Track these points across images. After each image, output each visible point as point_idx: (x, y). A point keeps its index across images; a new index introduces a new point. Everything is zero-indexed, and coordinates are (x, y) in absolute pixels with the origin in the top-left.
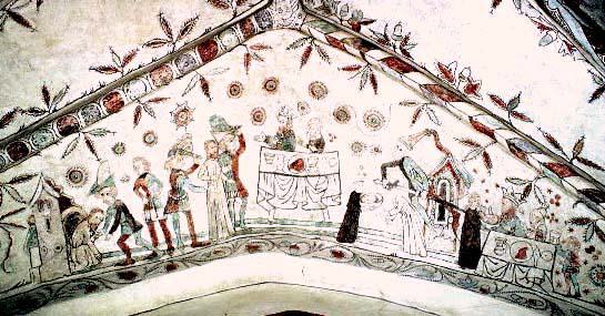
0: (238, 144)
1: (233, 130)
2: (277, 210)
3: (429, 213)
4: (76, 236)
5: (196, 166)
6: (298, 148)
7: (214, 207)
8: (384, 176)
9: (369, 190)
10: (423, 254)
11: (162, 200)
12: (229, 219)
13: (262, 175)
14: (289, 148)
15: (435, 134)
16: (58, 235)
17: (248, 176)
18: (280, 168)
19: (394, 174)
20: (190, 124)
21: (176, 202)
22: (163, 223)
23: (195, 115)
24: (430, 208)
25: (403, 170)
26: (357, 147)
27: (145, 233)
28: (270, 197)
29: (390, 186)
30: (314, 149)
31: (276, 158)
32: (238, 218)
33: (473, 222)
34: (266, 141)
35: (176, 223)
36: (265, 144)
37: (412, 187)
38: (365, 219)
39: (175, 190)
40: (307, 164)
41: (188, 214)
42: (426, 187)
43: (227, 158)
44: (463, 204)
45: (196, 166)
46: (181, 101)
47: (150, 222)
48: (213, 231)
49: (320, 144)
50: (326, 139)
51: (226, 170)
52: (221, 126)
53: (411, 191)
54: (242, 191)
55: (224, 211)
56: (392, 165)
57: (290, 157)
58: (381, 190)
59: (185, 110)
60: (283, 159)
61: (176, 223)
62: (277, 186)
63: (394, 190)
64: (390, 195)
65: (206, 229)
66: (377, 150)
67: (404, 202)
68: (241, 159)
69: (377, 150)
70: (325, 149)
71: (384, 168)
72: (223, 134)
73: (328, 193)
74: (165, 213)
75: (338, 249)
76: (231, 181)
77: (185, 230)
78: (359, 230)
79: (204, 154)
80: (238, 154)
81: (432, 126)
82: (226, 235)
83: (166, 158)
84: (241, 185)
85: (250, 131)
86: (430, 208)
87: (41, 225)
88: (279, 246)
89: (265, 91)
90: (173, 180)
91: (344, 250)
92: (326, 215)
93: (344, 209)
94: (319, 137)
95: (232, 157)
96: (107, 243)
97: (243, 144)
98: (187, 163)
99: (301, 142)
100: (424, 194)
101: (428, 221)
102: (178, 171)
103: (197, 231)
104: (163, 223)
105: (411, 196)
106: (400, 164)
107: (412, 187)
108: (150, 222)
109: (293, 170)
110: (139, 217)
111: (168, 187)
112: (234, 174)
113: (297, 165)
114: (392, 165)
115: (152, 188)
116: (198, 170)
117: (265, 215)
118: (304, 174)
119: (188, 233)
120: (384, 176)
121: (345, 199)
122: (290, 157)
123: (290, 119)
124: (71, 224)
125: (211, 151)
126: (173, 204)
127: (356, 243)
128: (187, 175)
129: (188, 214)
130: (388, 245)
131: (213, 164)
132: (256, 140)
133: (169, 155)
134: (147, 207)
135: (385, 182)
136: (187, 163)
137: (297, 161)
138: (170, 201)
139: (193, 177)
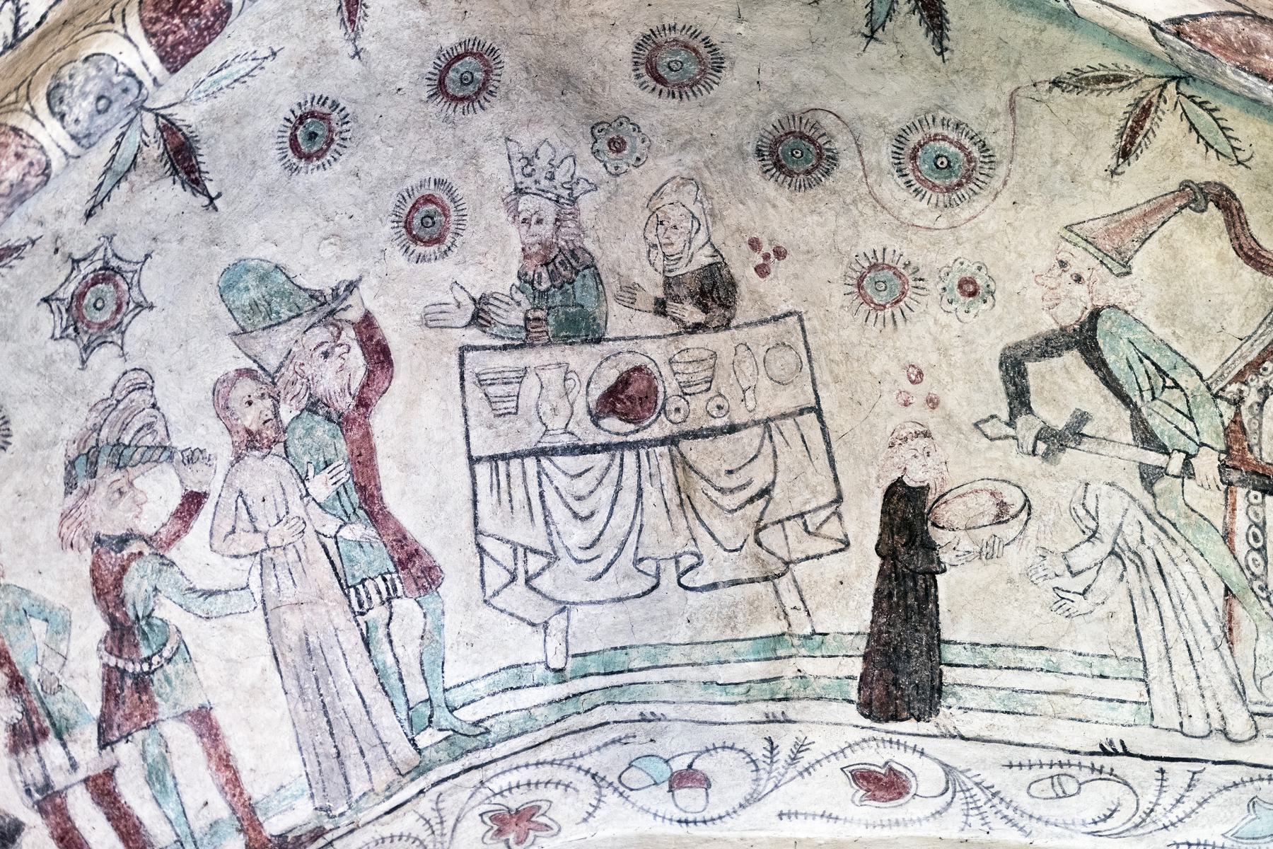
0: (357, 360)
1: (326, 306)
2: (577, 614)
3: (1241, 547)
5: (193, 502)
6: (618, 319)
7: (304, 666)
8: (1019, 399)
9: (966, 470)
10: (1239, 724)
11: (84, 695)
12: (379, 704)
13: (483, 470)
14: (582, 329)
15: (1224, 200)
17: (424, 492)
18: (557, 424)
19: (1064, 386)
20: (139, 327)
21: (142, 683)
22: (103, 789)
23: (152, 283)
24: (1241, 524)
25: (1097, 364)
26: (881, 285)
28: (535, 563)
29: (1055, 441)
30: (692, 314)
31: (531, 382)
32: (417, 691)
34: (479, 318)
35: (157, 775)
36: (474, 336)
37: (1147, 438)
38: (965, 599)
39: (122, 633)
40: (668, 386)
41: (203, 720)
42: (1211, 422)
43: (323, 430)
45: (193, 502)
46: (83, 239)
47: (49, 800)
49: (714, 292)
50: (742, 268)
51: (321, 487)
52: (266, 298)
53: (1154, 458)
54: (413, 566)
55: (351, 672)
56: (1049, 346)
57: (592, 368)
58: (1009, 461)
59: (107, 274)
60: (560, 382)
61: (157, 775)
62: (560, 514)
63: (1069, 457)
64: (1054, 483)
65: (292, 766)
66: (969, 288)
67: (1119, 510)
68: (384, 420)
69: (969, 288)
70: (745, 310)
71: (1013, 368)
72: (283, 337)
73: (781, 506)
74: (105, 743)
75: (875, 758)
76: (358, 530)
78: (950, 653)
79: (221, 446)
80: (363, 403)
81: (1206, 170)
82: (383, 775)
83: (58, 501)
84: (402, 538)
85: (401, 292)
86: (1241, 524)
88: (622, 789)
89: (438, 107)
90: (107, 590)
91: (902, 759)
92: (791, 599)
93: (864, 567)
94: (703, 258)
95: (342, 422)
97: (379, 356)
98: (158, 492)
99: (630, 293)
100: (1207, 464)
101: (1238, 581)
102: (123, 541)
103: (255, 789)
104: (103, 789)
105: (1149, 477)
106: (1084, 339)
107: (1147, 438)
108: (49, 800)
109: (612, 423)
111: (91, 627)
112: (368, 499)
113: (627, 397)
114: (1049, 346)
116: (208, 507)
117: (529, 647)
118: (657, 430)
119: (220, 808)
120: (1019, 399)
121: (864, 521)
122: (592, 368)
123: (567, 202)
125: (250, 419)
127: (949, 716)
128: (160, 545)
129: (203, 720)
130: (1090, 709)
131: (265, 476)
132: (427, 322)
133: (70, 485)
134: (25, 736)
135: (1027, 428)
136: (158, 492)
137: (624, 382)
138: (111, 694)
139: (194, 550)
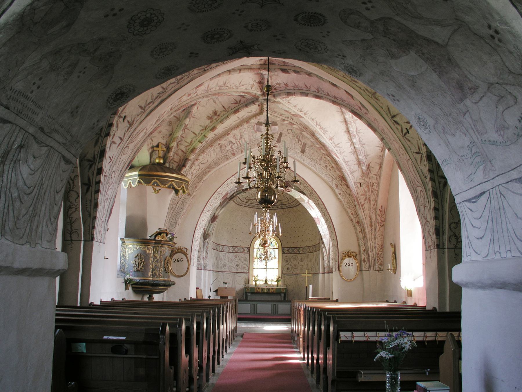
4: (222, 148)
16: (219, 149)
19: (290, 131)
27: (236, 145)
29: (289, 133)
33: (305, 145)
44: (303, 141)
47: (236, 142)
48: (250, 139)
77: (243, 141)
87: (215, 149)
90: (240, 134)
96: (229, 148)
108: (236, 142)
110: (234, 142)
115: (236, 137)
121: (279, 133)
124: (221, 147)
126: (241, 138)
139: (245, 132)
